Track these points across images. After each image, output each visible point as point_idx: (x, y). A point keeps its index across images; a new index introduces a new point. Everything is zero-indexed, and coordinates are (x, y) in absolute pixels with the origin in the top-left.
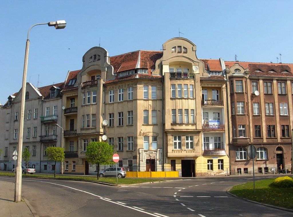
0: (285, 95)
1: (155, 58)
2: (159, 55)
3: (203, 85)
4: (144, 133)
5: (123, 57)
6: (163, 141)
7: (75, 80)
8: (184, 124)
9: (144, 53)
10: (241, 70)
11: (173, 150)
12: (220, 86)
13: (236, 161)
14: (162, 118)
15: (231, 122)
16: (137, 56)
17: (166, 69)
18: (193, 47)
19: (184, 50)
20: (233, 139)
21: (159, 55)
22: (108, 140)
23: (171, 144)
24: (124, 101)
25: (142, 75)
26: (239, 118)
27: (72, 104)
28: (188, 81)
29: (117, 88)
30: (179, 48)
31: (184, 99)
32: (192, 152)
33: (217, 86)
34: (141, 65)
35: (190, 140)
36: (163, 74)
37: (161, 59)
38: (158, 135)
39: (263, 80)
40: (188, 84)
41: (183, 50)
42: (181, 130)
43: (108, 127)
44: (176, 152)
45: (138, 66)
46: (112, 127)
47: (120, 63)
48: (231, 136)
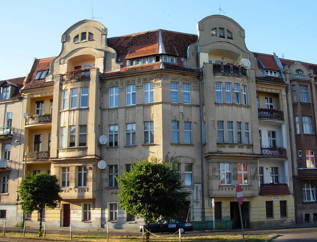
1: (184, 44)
4: (172, 158)
5: (131, 39)
6: (202, 172)
7: (47, 71)
10: (304, 72)
11: (219, 186)
12: (278, 92)
13: (303, 203)
14: (199, 135)
15: (295, 145)
17: (204, 58)
18: (240, 32)
19: (227, 34)
20: (299, 171)
22: (107, 170)
23: (217, 176)
24: (138, 105)
25: (170, 65)
26: (306, 140)
27: (39, 110)
28: (240, 79)
29: (124, 84)
30: (221, 31)
31: (236, 106)
32: (248, 189)
33: (274, 91)
35: (244, 170)
36: (201, 65)
37: (197, 44)
38: (195, 161)
40: (239, 84)
41: (227, 34)
42: (233, 155)
43: (107, 148)
44: (224, 189)
46: (114, 148)
47: (127, 47)
48: (296, 166)
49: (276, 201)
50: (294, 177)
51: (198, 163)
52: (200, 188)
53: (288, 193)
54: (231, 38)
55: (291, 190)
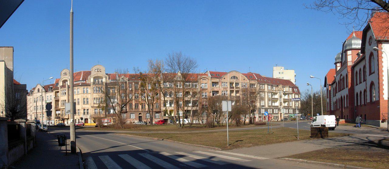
9: (84, 72)
34: (82, 79)
45: (81, 79)
54: (101, 72)
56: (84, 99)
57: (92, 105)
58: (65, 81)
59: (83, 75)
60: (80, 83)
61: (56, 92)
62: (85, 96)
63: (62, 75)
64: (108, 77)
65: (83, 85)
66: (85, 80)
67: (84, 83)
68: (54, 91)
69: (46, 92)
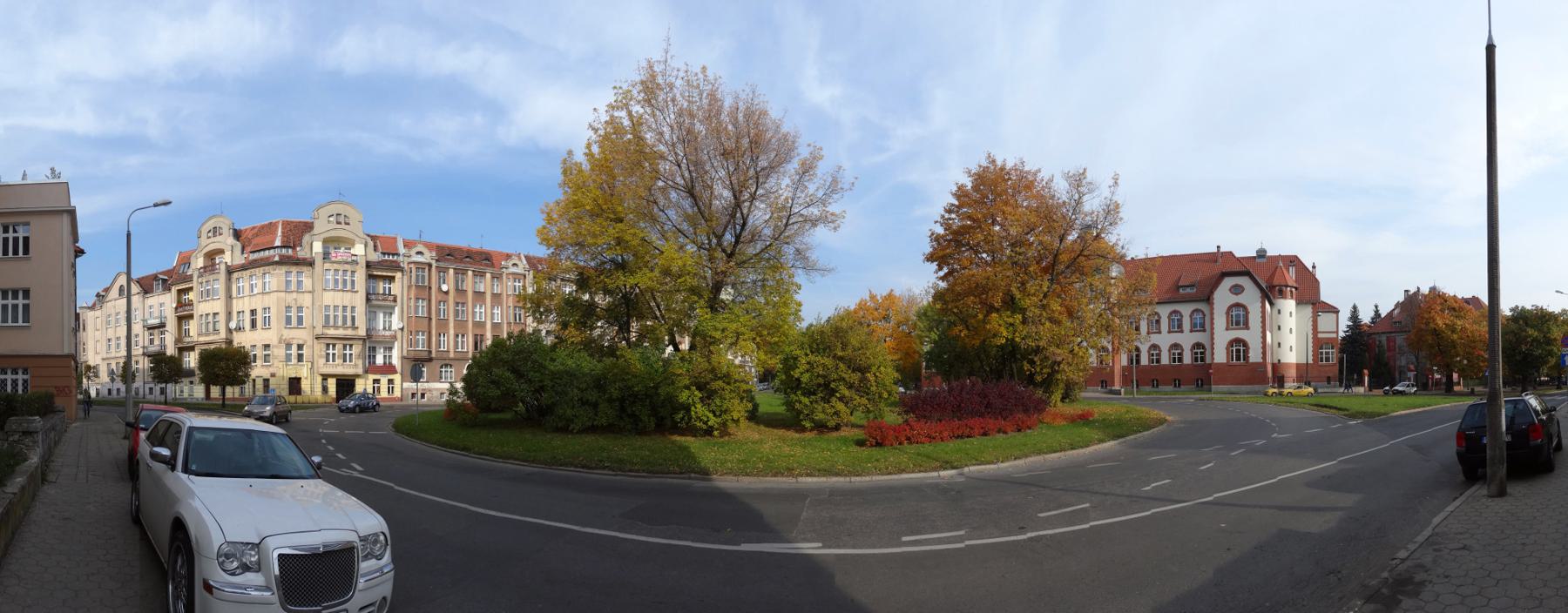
0: (484, 293)
2: (308, 227)
3: (370, 273)
8: (340, 327)
9: (286, 224)
16: (277, 228)
21: (308, 227)
34: (282, 242)
39: (454, 269)
45: (278, 243)
48: (405, 346)
49: (384, 380)
50: (403, 358)
51: (309, 343)
52: (310, 366)
53: (395, 372)
54: (348, 224)
55: (398, 368)
56: (288, 308)
57: (319, 331)
58: (211, 256)
59: (283, 233)
60: (275, 256)
61: (179, 292)
62: (290, 298)
63: (204, 236)
64: (371, 244)
65: (284, 261)
66: (294, 248)
67: (288, 257)
68: (174, 289)
69: (146, 292)
